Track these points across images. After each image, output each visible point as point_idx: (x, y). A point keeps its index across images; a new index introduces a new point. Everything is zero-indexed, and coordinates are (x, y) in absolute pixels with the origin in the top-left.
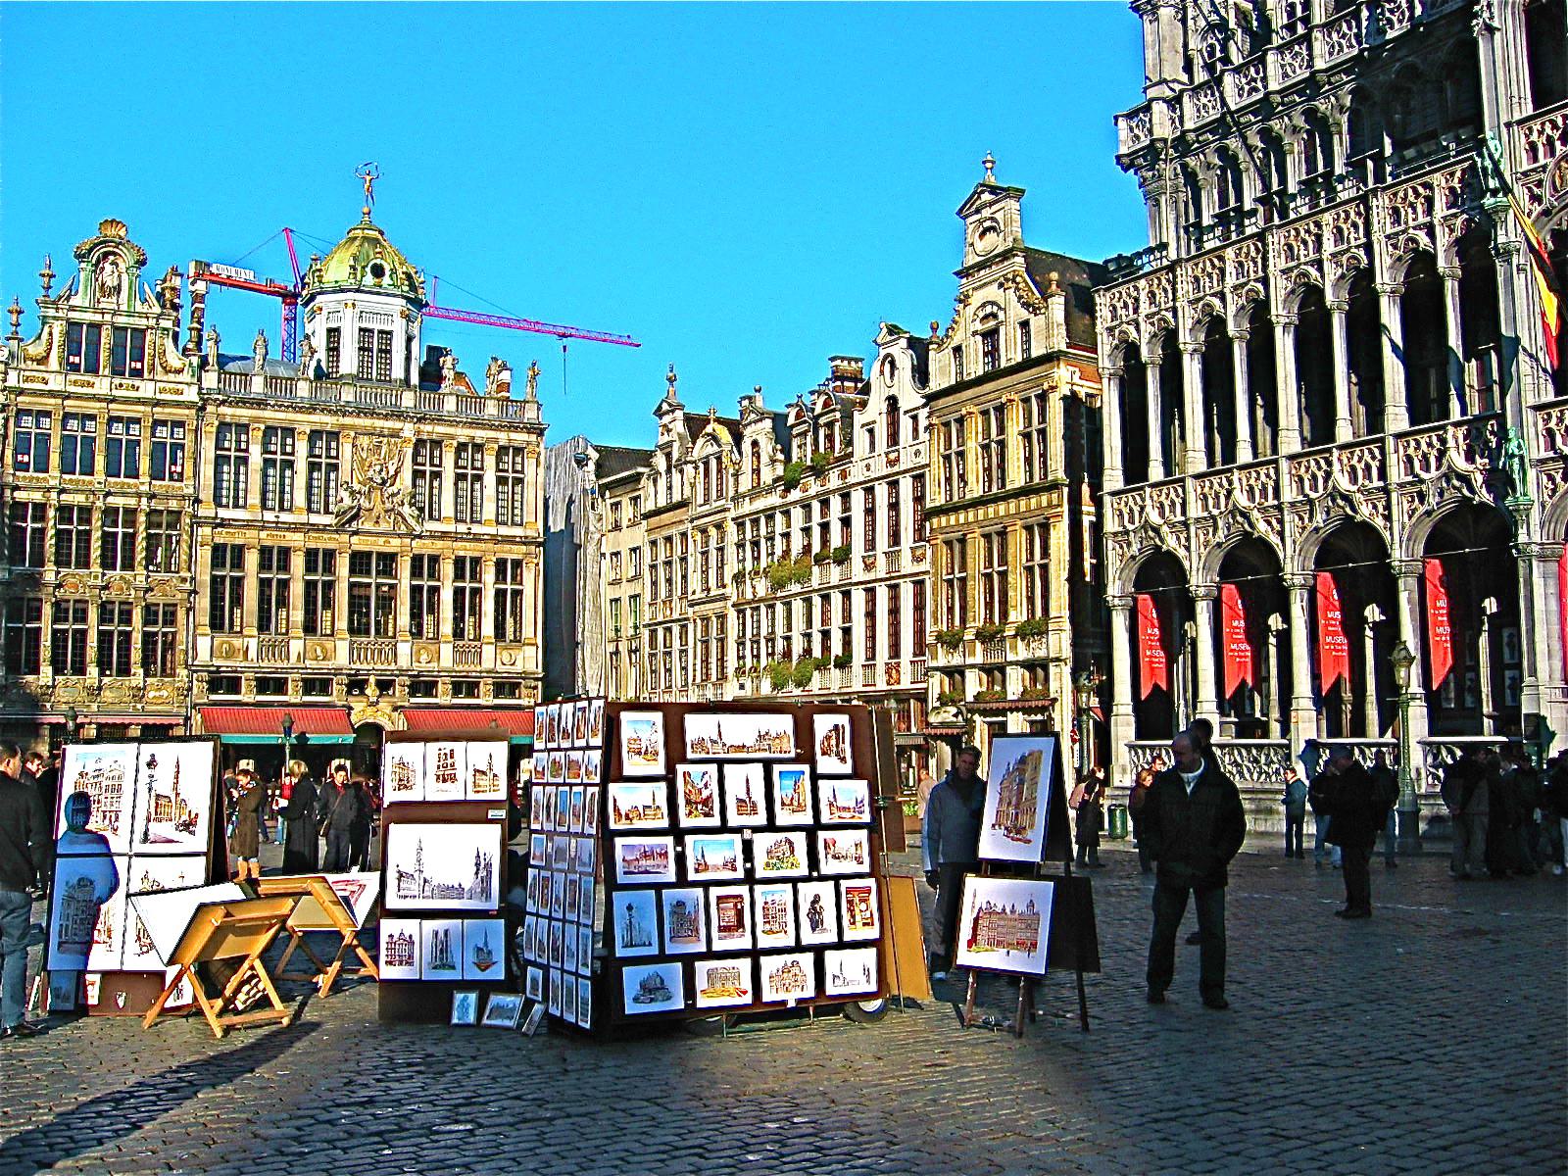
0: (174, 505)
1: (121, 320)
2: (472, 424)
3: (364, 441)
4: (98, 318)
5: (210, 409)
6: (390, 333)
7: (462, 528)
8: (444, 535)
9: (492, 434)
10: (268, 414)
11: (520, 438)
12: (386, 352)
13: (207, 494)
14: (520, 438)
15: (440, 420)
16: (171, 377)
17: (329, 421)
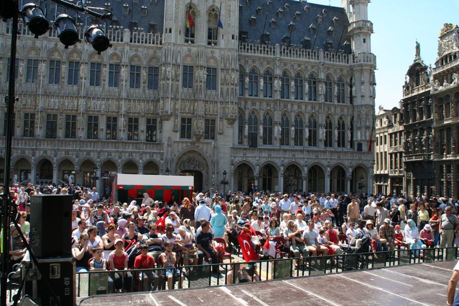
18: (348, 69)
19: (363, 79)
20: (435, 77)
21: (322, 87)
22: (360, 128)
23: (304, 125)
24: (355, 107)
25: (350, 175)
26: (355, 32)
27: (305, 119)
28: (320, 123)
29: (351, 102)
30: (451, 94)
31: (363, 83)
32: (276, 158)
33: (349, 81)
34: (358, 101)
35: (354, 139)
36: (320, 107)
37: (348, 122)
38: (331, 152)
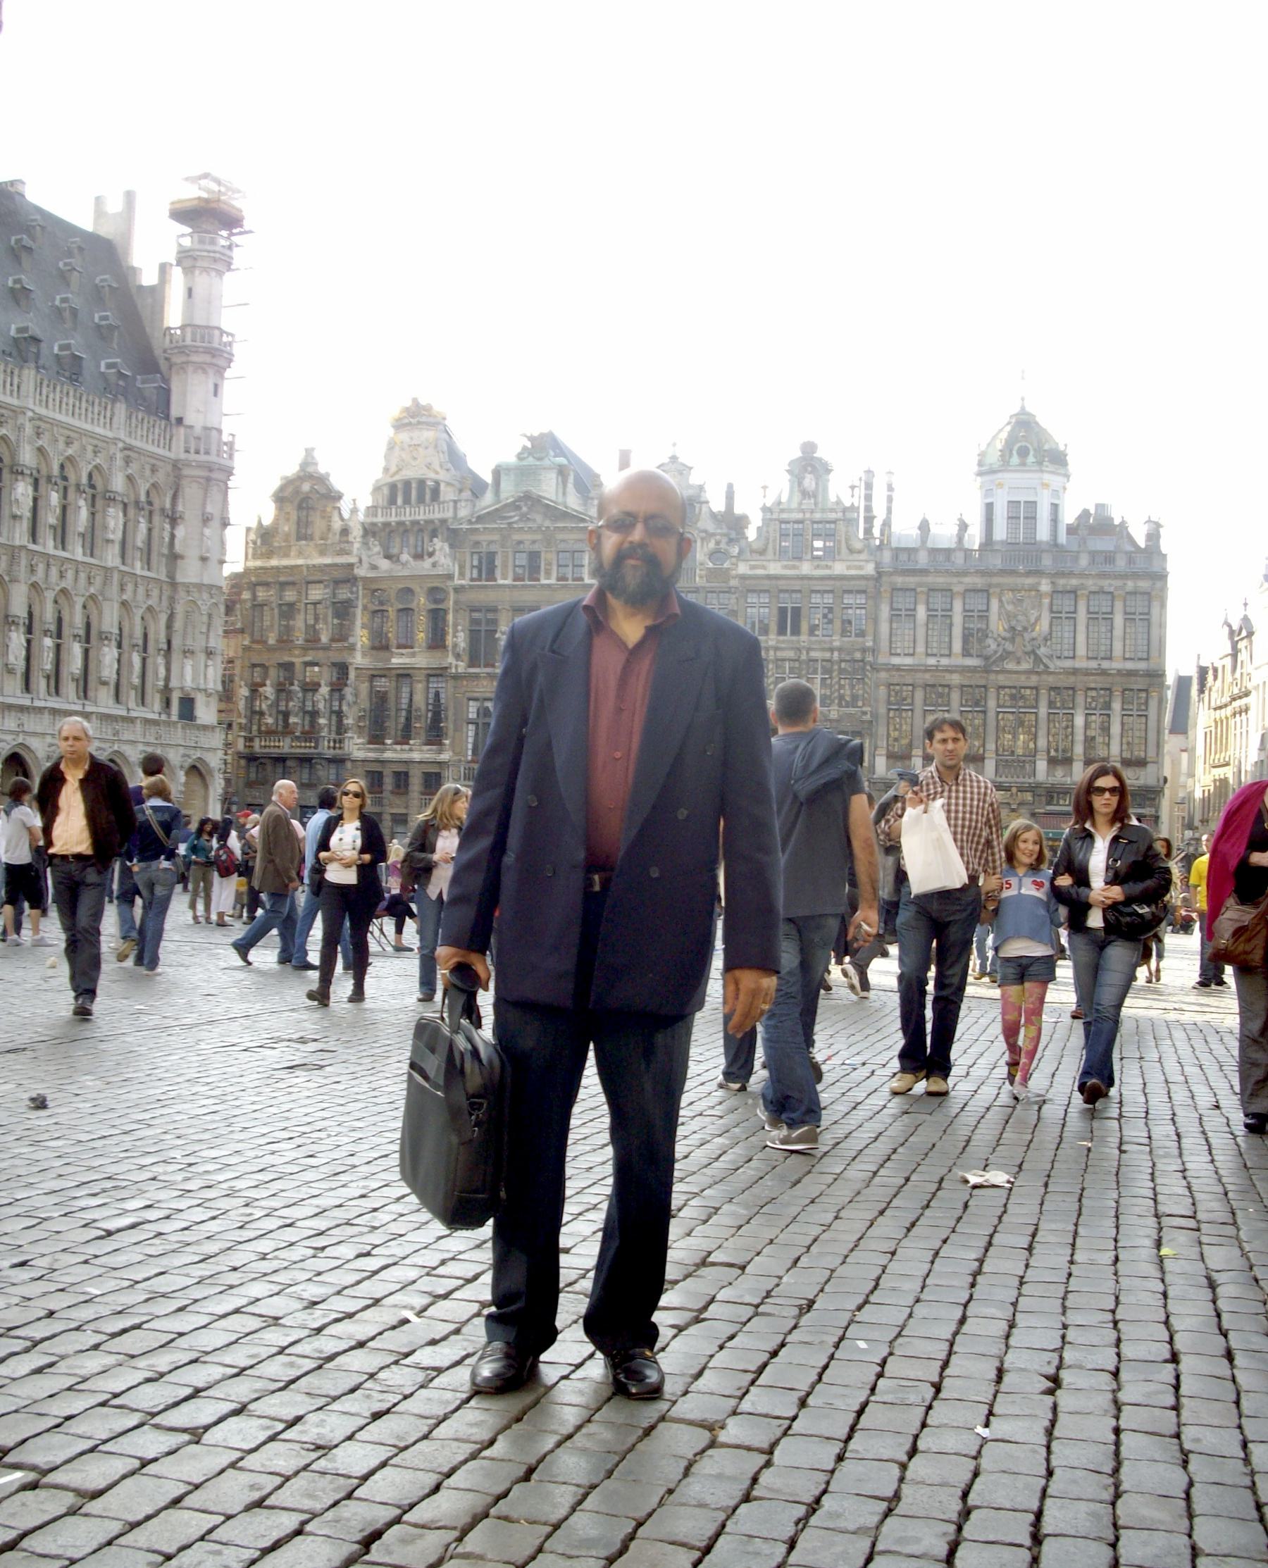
0: (858, 655)
1: (818, 516)
2: (1103, 575)
3: (1008, 596)
4: (800, 516)
5: (884, 579)
6: (1035, 503)
7: (1093, 664)
8: (1075, 672)
9: (1119, 583)
10: (930, 579)
11: (1144, 585)
12: (1032, 518)
13: (884, 645)
14: (1144, 585)
15: (1071, 574)
16: (856, 556)
17: (979, 581)
18: (169, 468)
19: (209, 509)
20: (369, 531)
21: (116, 518)
22: (188, 653)
23: (66, 631)
24: (182, 593)
25: (181, 792)
26: (194, 358)
27: (72, 614)
28: (105, 628)
29: (171, 575)
30: (417, 589)
31: (206, 520)
32: (35, 734)
33: (168, 505)
34: (189, 572)
35: (174, 683)
36: (106, 581)
37: (158, 632)
38: (147, 721)
